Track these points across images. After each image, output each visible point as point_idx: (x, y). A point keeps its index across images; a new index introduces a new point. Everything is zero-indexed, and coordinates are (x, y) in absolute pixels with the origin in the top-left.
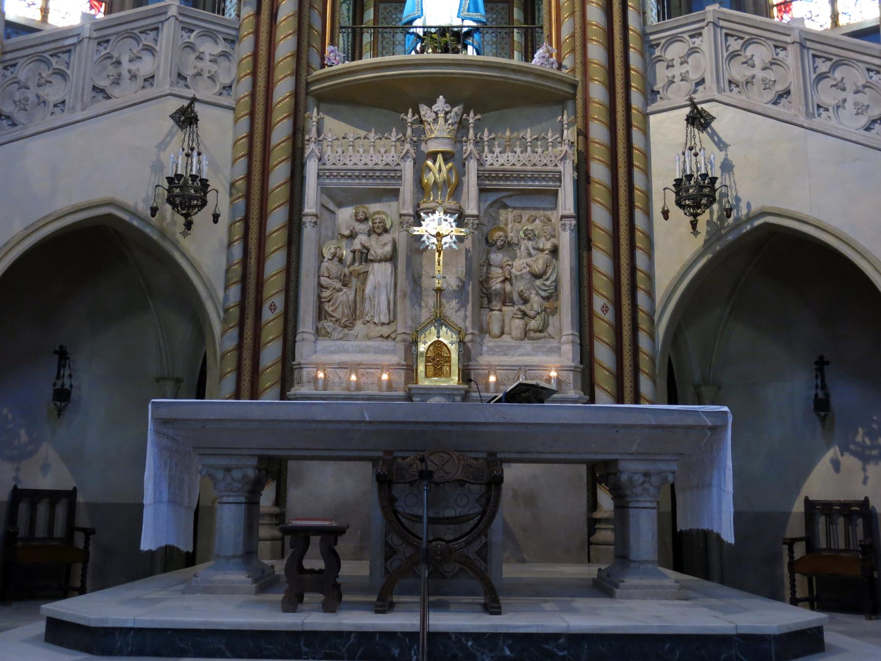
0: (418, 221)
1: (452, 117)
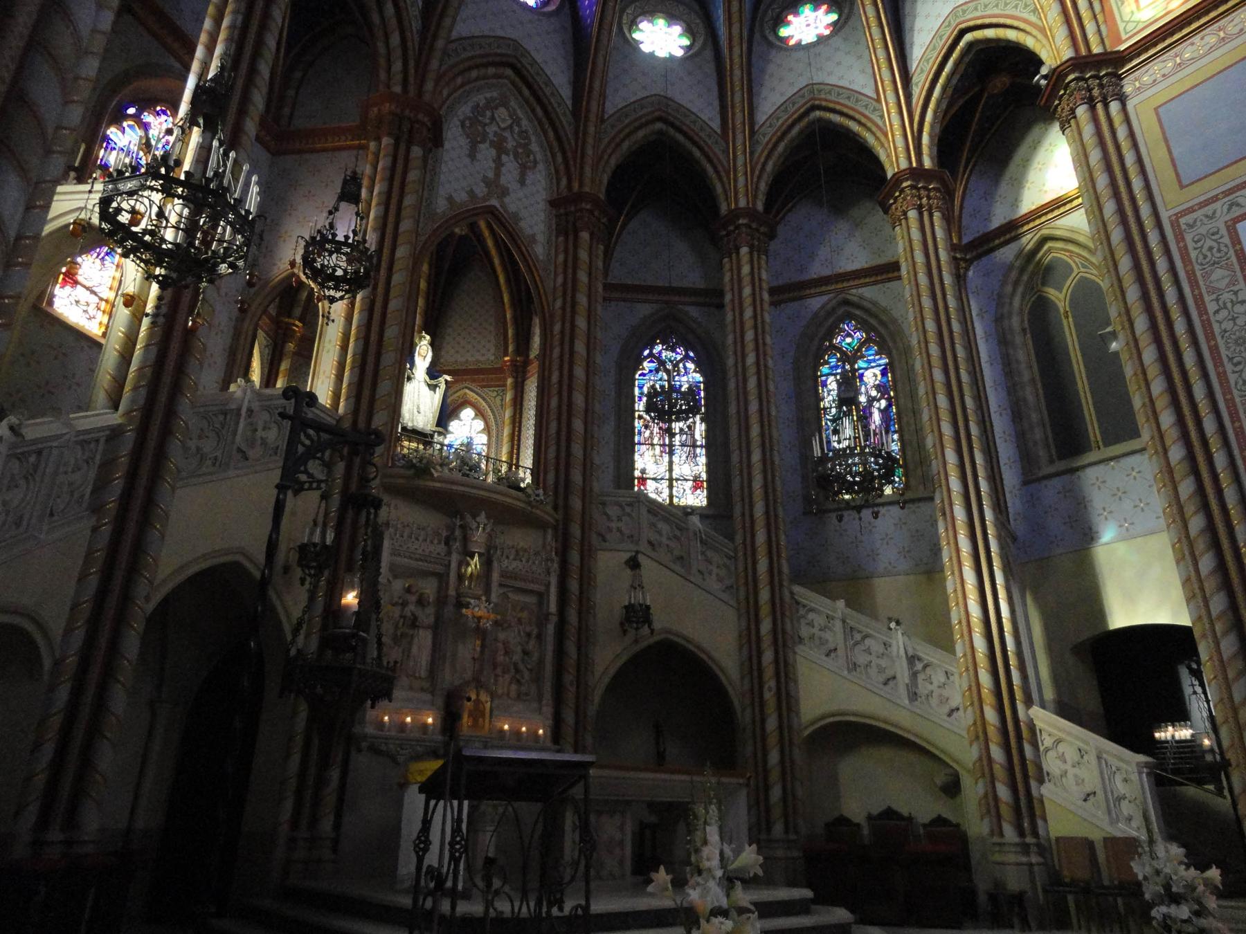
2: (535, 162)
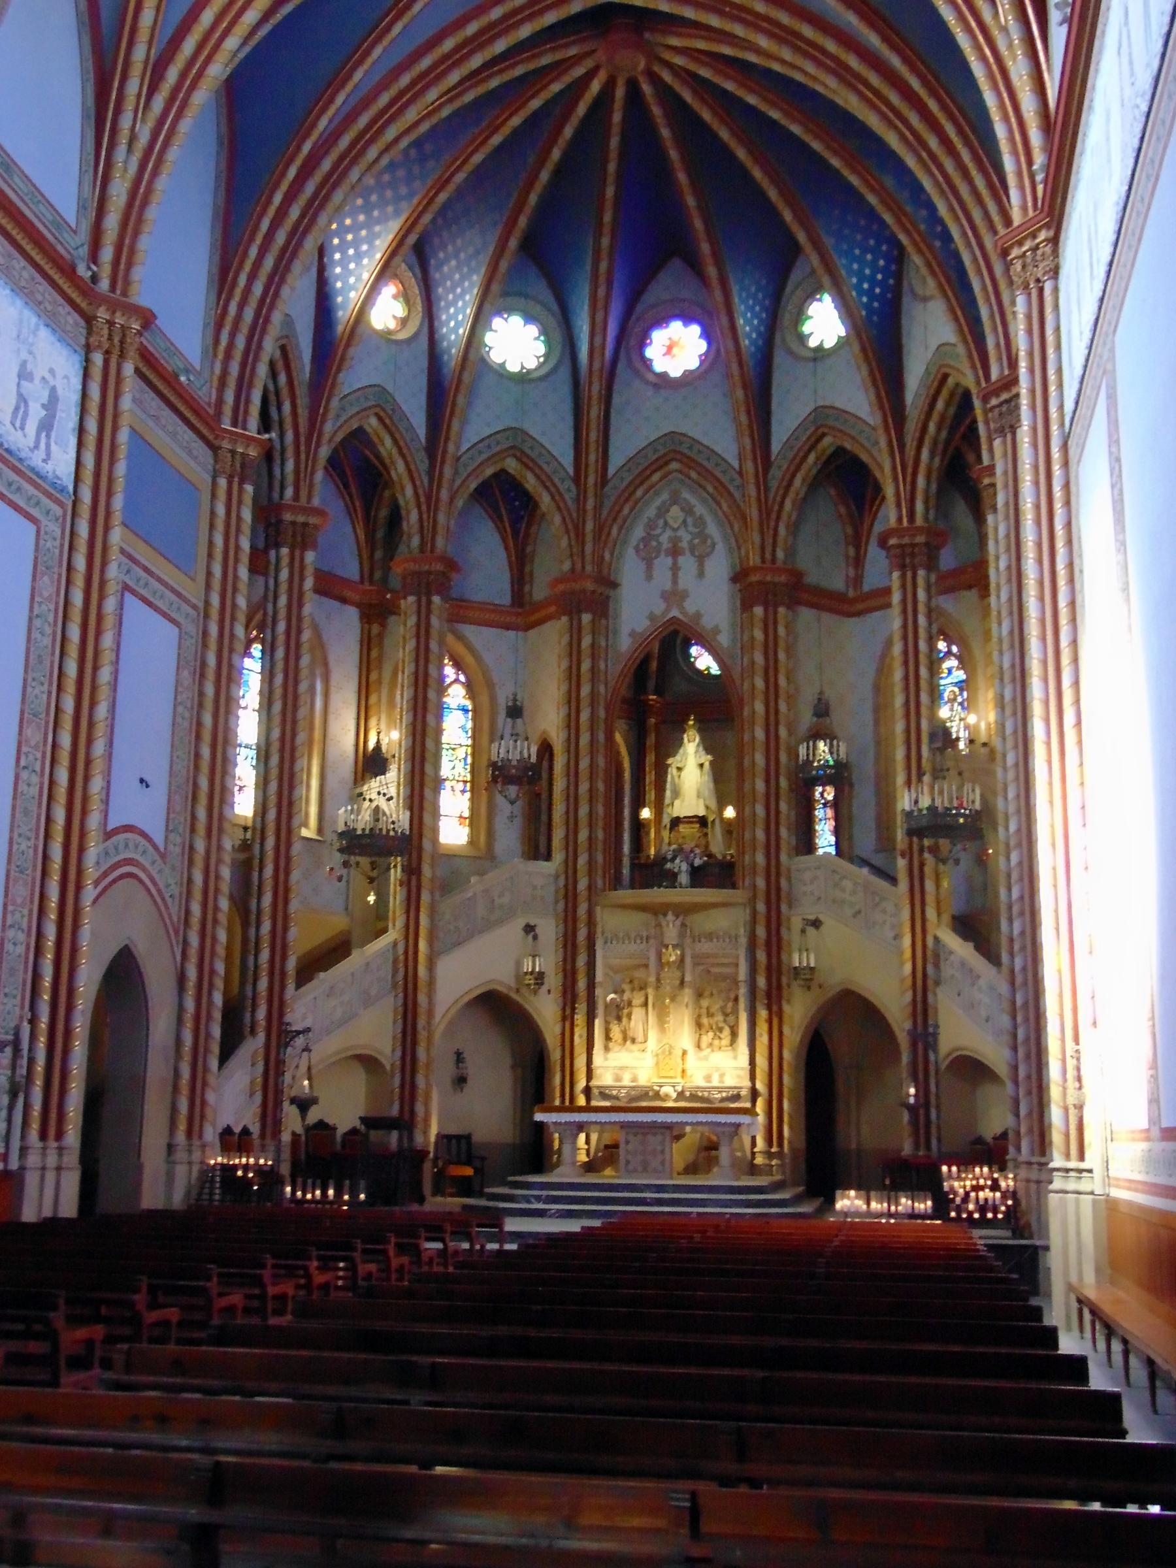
1: (678, 923)
2: (714, 545)
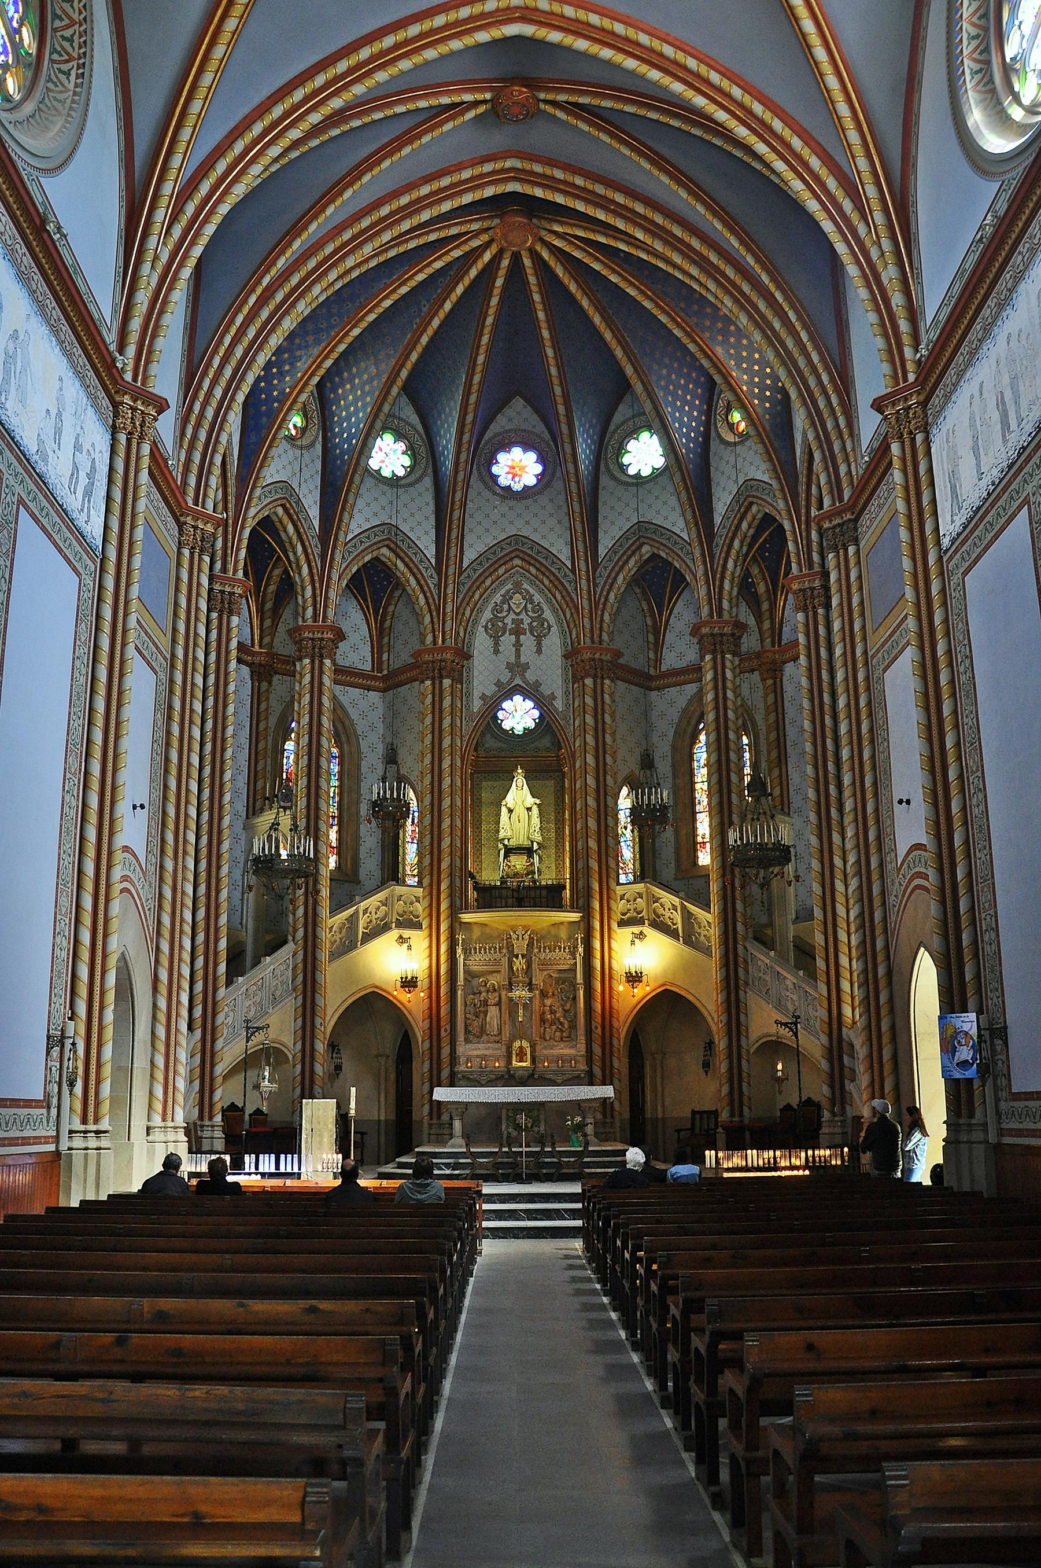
0: (511, 990)
2: (550, 627)
